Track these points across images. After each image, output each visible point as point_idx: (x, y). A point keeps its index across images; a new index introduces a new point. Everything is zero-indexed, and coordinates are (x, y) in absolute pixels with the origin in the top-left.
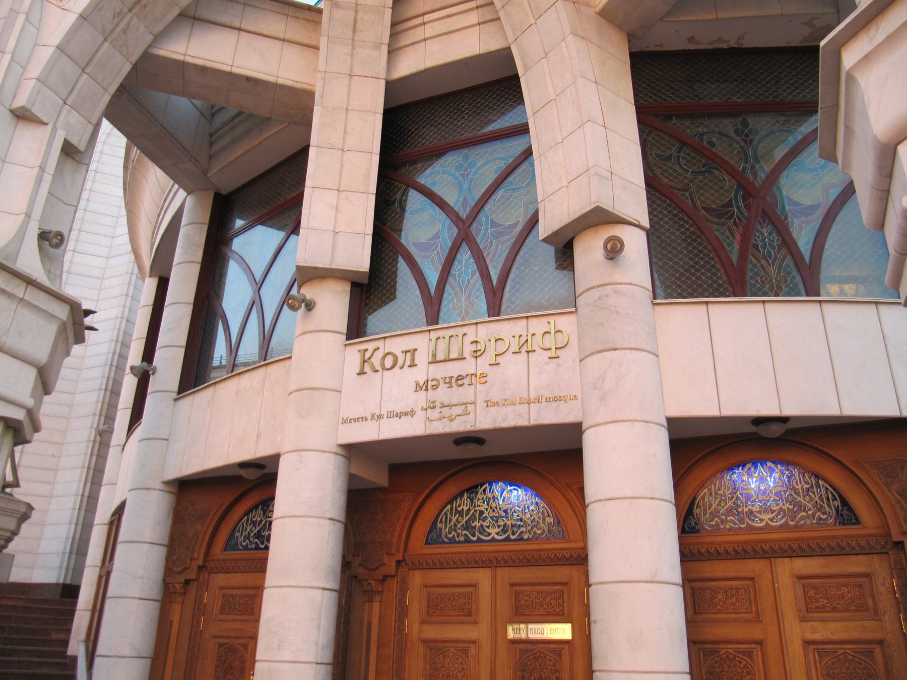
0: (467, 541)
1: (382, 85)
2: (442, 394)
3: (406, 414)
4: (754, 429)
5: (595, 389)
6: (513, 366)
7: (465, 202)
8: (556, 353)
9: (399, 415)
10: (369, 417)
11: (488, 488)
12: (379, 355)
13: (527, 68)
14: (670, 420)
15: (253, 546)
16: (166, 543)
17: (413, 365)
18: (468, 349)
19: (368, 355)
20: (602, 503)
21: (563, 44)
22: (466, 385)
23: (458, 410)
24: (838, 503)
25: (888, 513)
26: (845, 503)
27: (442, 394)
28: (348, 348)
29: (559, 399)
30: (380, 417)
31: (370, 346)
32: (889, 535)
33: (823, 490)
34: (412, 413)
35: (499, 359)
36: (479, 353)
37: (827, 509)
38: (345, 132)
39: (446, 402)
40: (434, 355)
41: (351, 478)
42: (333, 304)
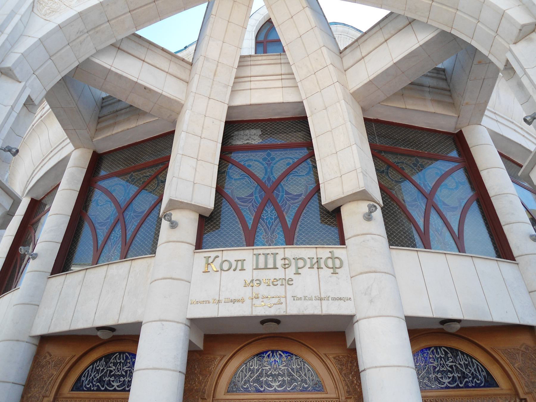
2: (262, 290)
3: (238, 301)
4: (441, 326)
5: (365, 294)
7: (269, 179)
8: (335, 270)
9: (234, 301)
10: (211, 301)
11: (271, 354)
12: (218, 261)
14: (406, 317)
15: (95, 388)
16: (24, 383)
17: (242, 269)
19: (211, 260)
20: (378, 369)
21: (338, 104)
22: (279, 286)
24: (484, 373)
25: (515, 380)
28: (196, 255)
29: (340, 299)
31: (213, 255)
32: (517, 394)
33: (475, 365)
34: (242, 301)
35: (300, 271)
36: (287, 266)
37: (479, 377)
38: (203, 128)
41: (191, 343)
42: (188, 224)
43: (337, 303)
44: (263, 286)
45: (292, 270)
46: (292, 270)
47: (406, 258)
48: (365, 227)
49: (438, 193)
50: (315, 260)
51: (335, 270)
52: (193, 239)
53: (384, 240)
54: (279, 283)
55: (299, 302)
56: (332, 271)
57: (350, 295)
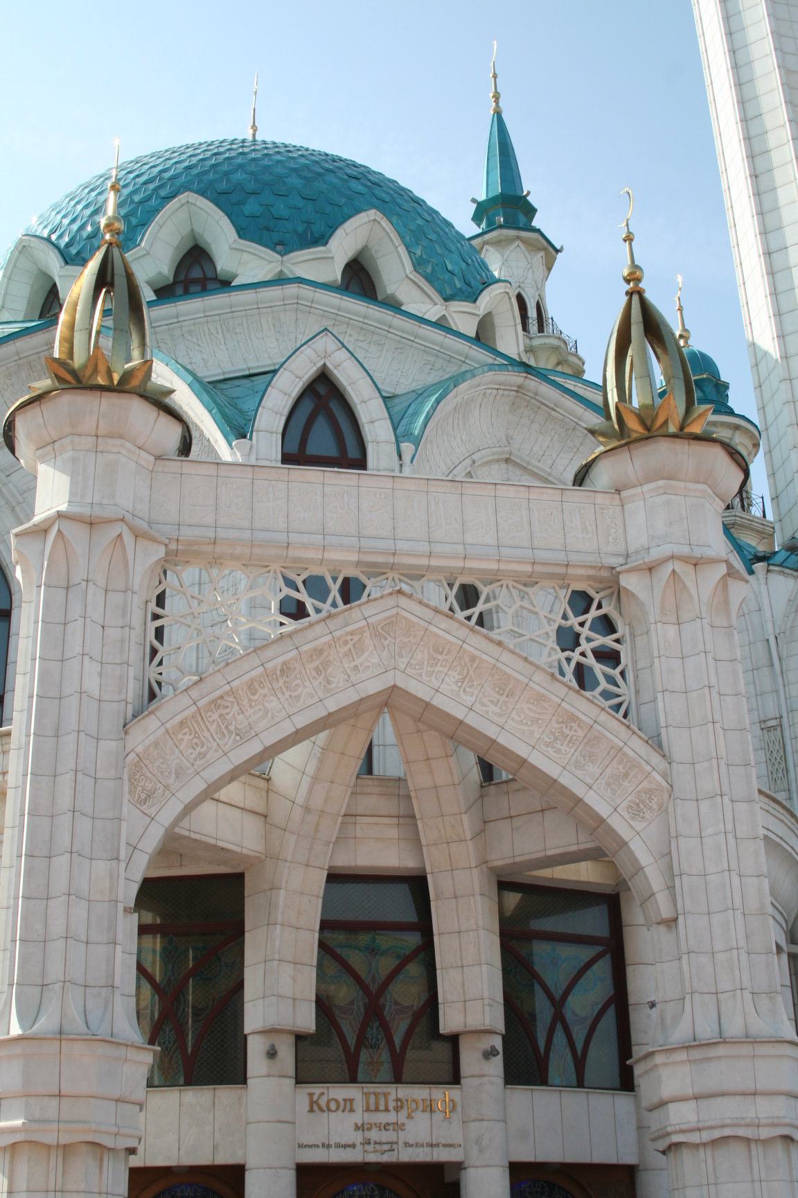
1: (326, 873)
6: (422, 1119)
7: (374, 978)
9: (345, 1146)
13: (438, 898)
17: (352, 1110)
18: (392, 1105)
19: (315, 1098)
23: (387, 1147)
27: (374, 1135)
29: (451, 1146)
30: (329, 1146)
34: (353, 1146)
43: (448, 1149)
47: (522, 1096)
48: (483, 1071)
49: (570, 998)
53: (500, 1081)
55: (410, 1149)
57: (460, 1141)
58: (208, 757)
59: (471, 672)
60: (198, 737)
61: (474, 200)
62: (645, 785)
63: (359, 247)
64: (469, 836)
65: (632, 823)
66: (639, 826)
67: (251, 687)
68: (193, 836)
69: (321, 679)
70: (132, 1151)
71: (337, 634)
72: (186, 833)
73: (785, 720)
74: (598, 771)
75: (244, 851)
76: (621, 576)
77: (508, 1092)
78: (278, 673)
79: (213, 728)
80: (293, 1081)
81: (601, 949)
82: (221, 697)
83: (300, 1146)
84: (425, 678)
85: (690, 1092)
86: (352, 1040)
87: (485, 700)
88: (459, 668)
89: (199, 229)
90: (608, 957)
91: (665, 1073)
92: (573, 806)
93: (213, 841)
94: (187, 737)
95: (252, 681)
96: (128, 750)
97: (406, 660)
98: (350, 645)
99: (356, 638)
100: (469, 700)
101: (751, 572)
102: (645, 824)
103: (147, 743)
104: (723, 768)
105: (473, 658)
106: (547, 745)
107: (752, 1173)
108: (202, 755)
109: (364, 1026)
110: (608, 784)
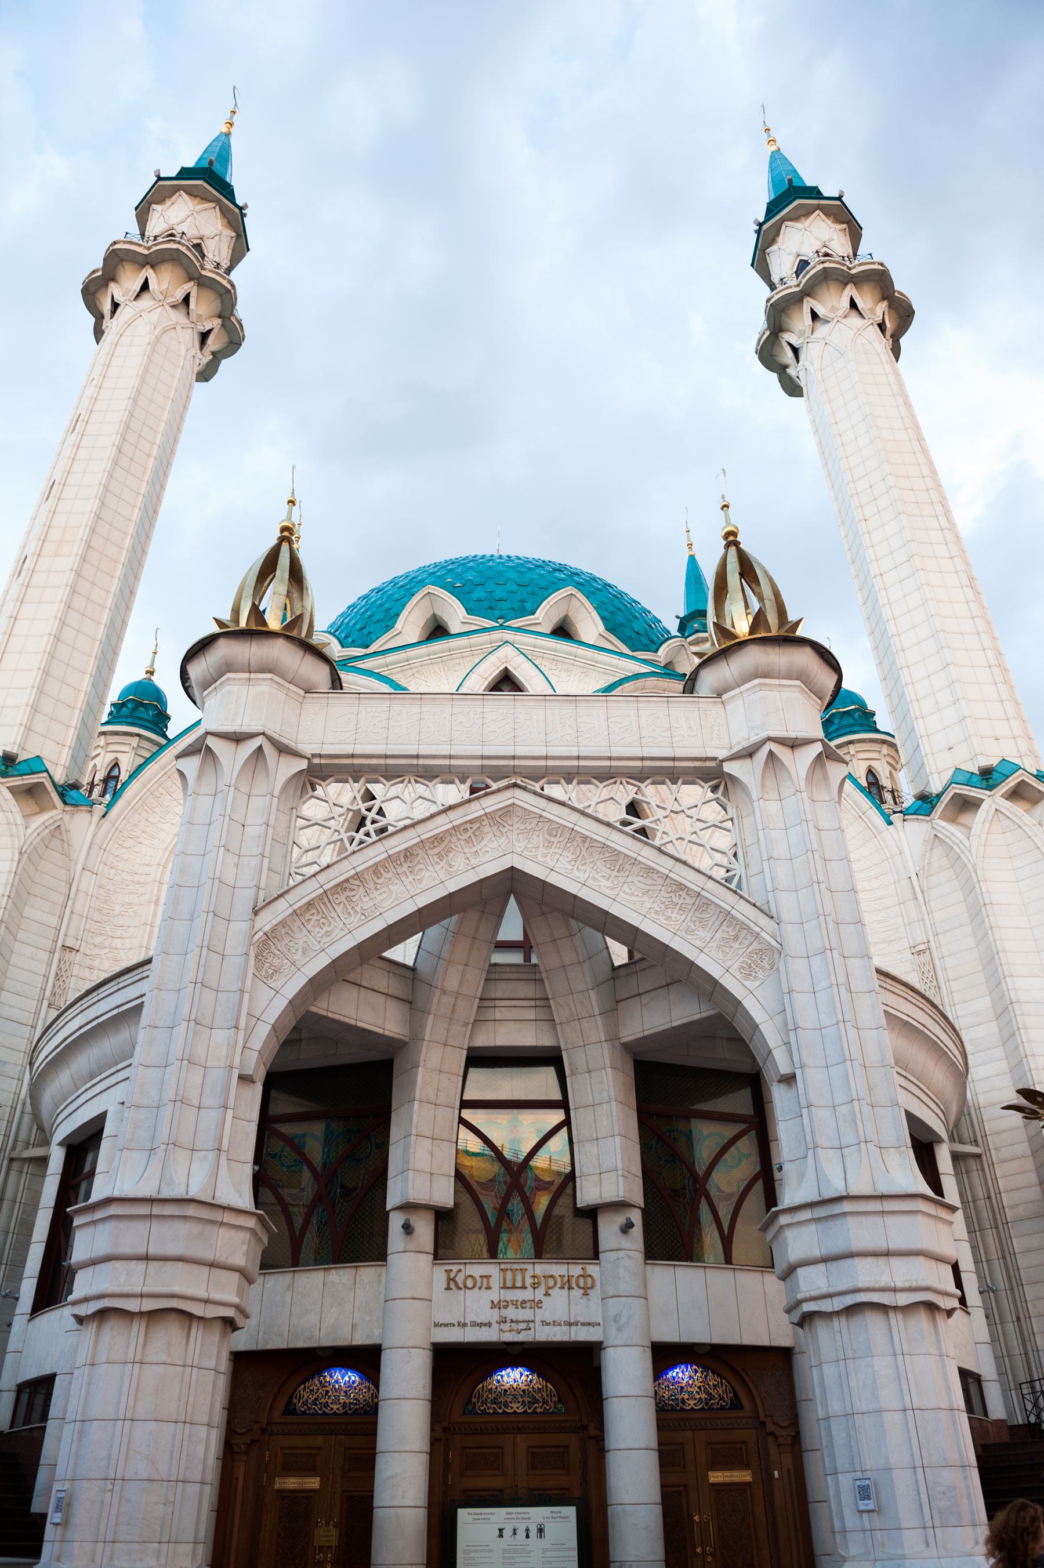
0: (495, 1413)
1: (465, 1052)
2: (511, 1313)
3: (485, 1325)
6: (559, 1296)
8: (586, 1291)
9: (480, 1325)
13: (572, 1074)
14: (652, 1343)
17: (489, 1288)
18: (529, 1281)
19: (452, 1275)
23: (523, 1326)
26: (736, 1395)
27: (511, 1313)
28: (436, 1268)
29: (589, 1324)
30: (465, 1325)
31: (455, 1268)
32: (758, 1417)
34: (489, 1325)
35: (550, 1291)
39: (514, 1319)
40: (505, 1283)
43: (586, 1328)
44: (511, 1308)
45: (541, 1290)
46: (541, 1290)
48: (622, 1245)
49: (714, 1174)
50: (566, 1279)
51: (586, 1291)
52: (430, 1247)
53: (639, 1256)
54: (528, 1305)
55: (547, 1328)
56: (582, 1291)
58: (333, 935)
59: (584, 852)
60: (326, 918)
61: (677, 617)
62: (755, 946)
63: (562, 615)
64: (597, 1012)
65: (745, 982)
66: (751, 984)
67: (376, 869)
68: (330, 1015)
69: (442, 864)
70: (230, 1324)
71: (456, 823)
72: (324, 1013)
73: (932, 945)
74: (709, 935)
75: (386, 1033)
76: (724, 764)
77: (649, 1267)
78: (402, 859)
79: (339, 909)
80: (431, 1257)
81: (745, 1126)
82: (347, 881)
83: (436, 1325)
84: (540, 859)
85: (817, 1253)
86: (492, 1218)
87: (597, 876)
88: (572, 849)
89: (439, 613)
90: (753, 1133)
91: (790, 1235)
92: (708, 987)
93: (353, 1022)
94: (315, 918)
95: (376, 864)
96: (256, 929)
97: (522, 844)
98: (470, 833)
99: (476, 826)
100: (582, 877)
101: (890, 823)
102: (759, 983)
103: (275, 922)
104: (831, 925)
105: (585, 838)
106: (657, 912)
107: (893, 1345)
108: (328, 934)
109: (506, 1200)
110: (719, 947)
